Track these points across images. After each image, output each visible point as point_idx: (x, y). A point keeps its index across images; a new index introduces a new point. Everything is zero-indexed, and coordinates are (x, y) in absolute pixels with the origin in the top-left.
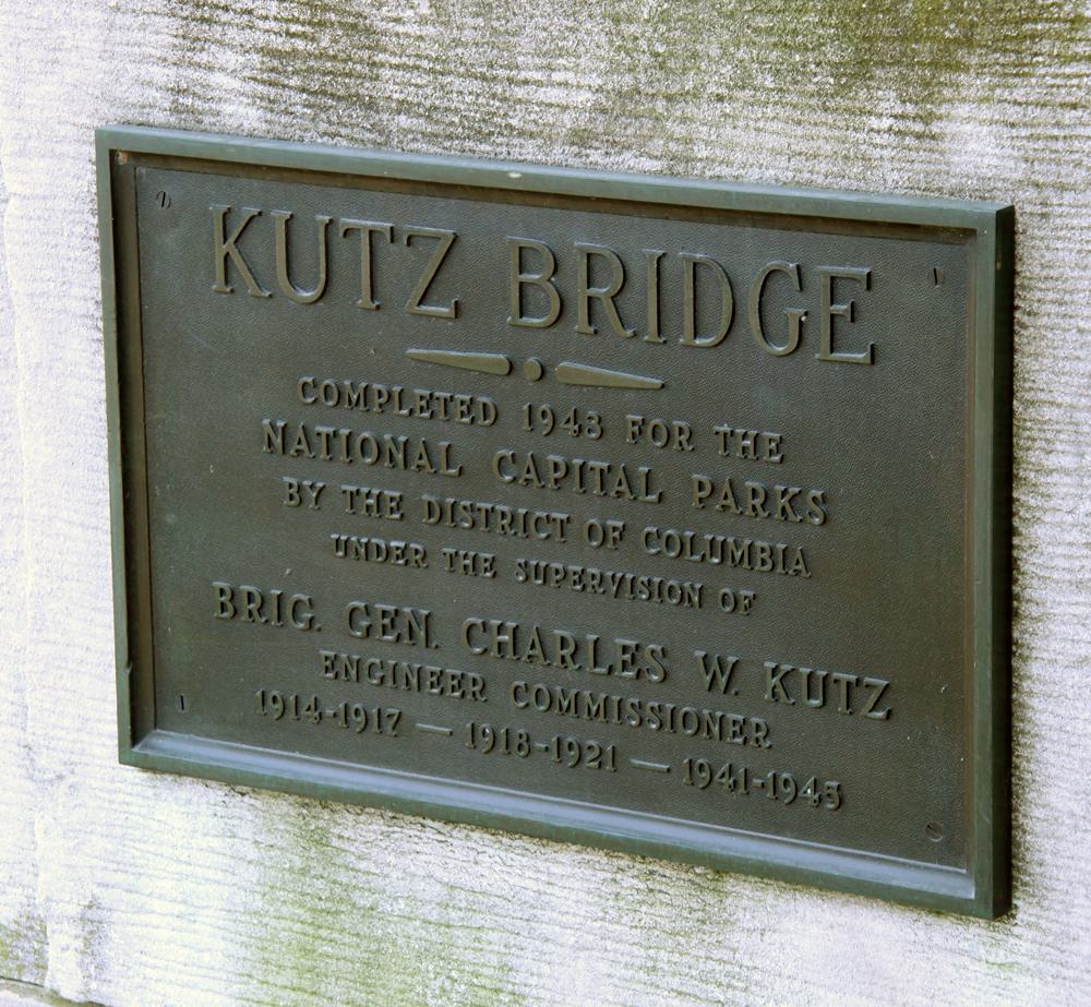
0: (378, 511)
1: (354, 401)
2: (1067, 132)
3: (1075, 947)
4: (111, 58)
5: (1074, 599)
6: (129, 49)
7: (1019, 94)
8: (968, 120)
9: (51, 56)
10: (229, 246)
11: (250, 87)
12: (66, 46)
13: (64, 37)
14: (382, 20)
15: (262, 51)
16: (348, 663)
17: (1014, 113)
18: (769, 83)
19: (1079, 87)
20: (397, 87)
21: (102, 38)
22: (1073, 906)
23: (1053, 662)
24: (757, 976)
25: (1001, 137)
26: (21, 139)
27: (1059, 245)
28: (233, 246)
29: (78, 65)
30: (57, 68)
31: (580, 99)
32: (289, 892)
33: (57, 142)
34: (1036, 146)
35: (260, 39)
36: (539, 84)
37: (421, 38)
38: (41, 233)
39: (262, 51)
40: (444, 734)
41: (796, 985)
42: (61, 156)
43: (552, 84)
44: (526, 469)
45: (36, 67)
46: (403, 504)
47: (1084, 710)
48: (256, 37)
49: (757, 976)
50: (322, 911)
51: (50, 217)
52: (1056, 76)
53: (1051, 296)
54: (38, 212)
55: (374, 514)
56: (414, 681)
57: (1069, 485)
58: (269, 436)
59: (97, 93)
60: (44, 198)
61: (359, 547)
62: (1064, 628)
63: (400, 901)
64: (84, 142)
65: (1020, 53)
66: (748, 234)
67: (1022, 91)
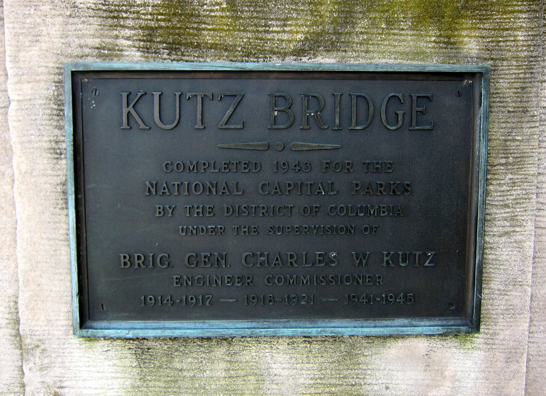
0: (202, 214)
1: (191, 169)
2: (505, 39)
3: (497, 337)
4: (66, 37)
5: (503, 211)
6: (76, 32)
7: (487, 26)
8: (466, 36)
9: (35, 39)
10: (131, 108)
11: (137, 44)
12: (43, 33)
13: (43, 30)
14: (204, 11)
15: (141, 28)
16: (187, 279)
17: (485, 33)
18: (383, 26)
19: (509, 22)
20: (210, 38)
21: (62, 29)
22: (498, 322)
23: (494, 235)
24: (369, 372)
25: (479, 42)
26: (18, 76)
27: (501, 81)
28: (132, 109)
29: (49, 41)
30: (38, 44)
31: (298, 37)
32: (153, 376)
33: (37, 75)
34: (492, 45)
35: (143, 23)
36: (278, 32)
37: (222, 17)
38: (28, 115)
39: (141, 28)
40: (234, 302)
41: (386, 372)
42: (39, 81)
43: (284, 32)
44: (275, 187)
45: (27, 44)
46: (214, 210)
47: (505, 251)
48: (141, 22)
49: (369, 372)
50: (169, 381)
51: (32, 108)
52: (500, 19)
53: (498, 99)
54: (26, 106)
55: (201, 215)
56: (219, 282)
57: (503, 170)
58: (149, 188)
59: (59, 52)
60: (30, 100)
61: (193, 230)
62: (499, 222)
63: (207, 371)
64: (51, 74)
65: (487, 11)
66: (379, 83)
67: (487, 25)
